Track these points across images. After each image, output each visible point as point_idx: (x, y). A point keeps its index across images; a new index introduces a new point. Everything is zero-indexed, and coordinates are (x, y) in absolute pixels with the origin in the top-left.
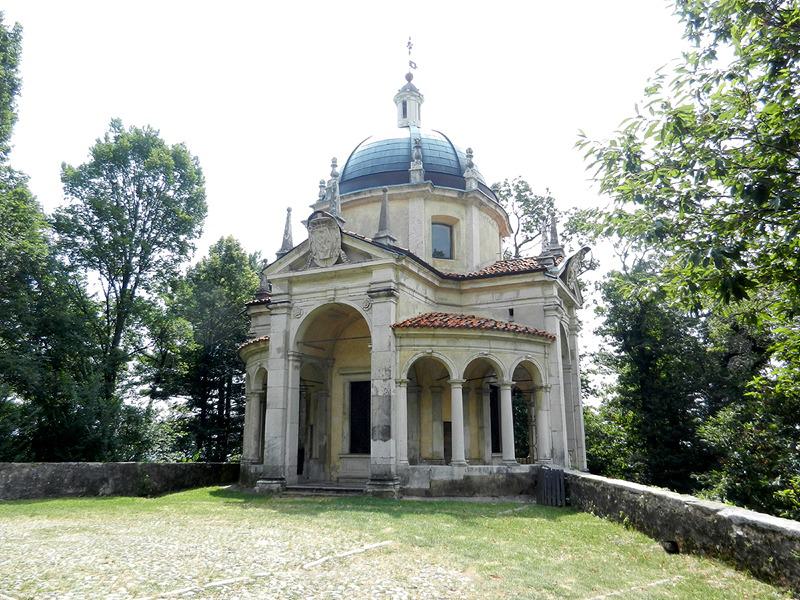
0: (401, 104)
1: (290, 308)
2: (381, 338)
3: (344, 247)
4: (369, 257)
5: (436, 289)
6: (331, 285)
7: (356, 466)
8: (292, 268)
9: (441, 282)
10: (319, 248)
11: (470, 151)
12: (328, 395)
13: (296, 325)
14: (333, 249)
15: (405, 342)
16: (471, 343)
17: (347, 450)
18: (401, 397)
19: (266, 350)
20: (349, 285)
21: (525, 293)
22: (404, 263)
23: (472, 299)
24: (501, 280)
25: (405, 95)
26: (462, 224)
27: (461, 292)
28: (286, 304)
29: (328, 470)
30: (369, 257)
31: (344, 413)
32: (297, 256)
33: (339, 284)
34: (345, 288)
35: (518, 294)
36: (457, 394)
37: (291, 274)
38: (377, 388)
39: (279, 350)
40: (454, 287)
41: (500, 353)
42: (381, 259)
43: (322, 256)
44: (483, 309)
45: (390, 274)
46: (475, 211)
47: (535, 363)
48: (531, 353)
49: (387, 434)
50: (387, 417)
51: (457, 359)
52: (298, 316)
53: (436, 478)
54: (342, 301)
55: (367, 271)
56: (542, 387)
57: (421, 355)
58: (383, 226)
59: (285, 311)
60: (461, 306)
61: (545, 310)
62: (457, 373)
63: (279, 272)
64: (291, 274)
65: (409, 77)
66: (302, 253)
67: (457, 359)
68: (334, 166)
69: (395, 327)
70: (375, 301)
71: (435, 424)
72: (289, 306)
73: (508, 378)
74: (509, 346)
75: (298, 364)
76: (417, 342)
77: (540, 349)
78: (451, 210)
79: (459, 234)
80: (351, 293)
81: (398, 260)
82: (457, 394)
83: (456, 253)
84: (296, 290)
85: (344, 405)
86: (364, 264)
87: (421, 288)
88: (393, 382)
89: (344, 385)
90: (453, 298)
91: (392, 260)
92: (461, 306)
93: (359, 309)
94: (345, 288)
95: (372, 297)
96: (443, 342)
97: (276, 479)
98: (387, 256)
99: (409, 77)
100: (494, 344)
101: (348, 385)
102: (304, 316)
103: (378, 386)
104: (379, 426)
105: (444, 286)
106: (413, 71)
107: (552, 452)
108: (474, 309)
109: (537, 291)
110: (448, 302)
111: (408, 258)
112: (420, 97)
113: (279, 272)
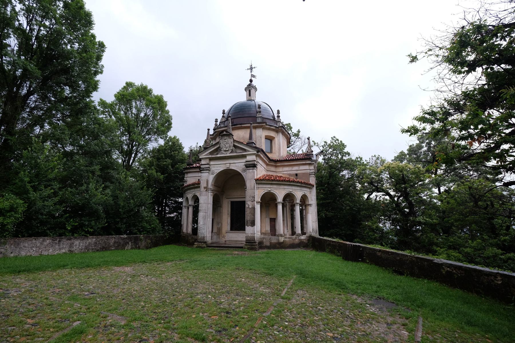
0: (248, 91)
1: (210, 170)
2: (250, 183)
3: (234, 146)
4: (245, 150)
5: (267, 165)
7: (239, 237)
9: (269, 162)
10: (223, 146)
11: (278, 112)
12: (221, 207)
14: (230, 147)
15: (260, 186)
18: (258, 207)
19: (199, 187)
21: (302, 167)
22: (260, 153)
23: (280, 169)
24: (292, 162)
25: (250, 88)
26: (276, 139)
27: (276, 166)
28: (208, 169)
29: (221, 237)
31: (228, 214)
32: (213, 149)
33: (231, 161)
35: (299, 168)
36: (280, 207)
37: (210, 156)
38: (249, 204)
39: (205, 188)
40: (274, 164)
41: (296, 191)
42: (249, 151)
43: (225, 149)
45: (253, 158)
46: (281, 135)
47: (307, 195)
48: (306, 191)
49: (253, 224)
50: (253, 217)
51: (280, 193)
52: (213, 174)
53: (272, 242)
55: (244, 156)
56: (309, 205)
57: (266, 191)
58: (251, 137)
59: (208, 171)
60: (276, 172)
61: (310, 175)
62: (280, 199)
63: (205, 156)
65: (251, 81)
66: (215, 148)
67: (280, 193)
68: (224, 113)
69: (256, 180)
71: (267, 219)
72: (208, 169)
73: (298, 201)
74: (298, 188)
75: (212, 194)
77: (308, 190)
78: (272, 134)
79: (275, 143)
80: (238, 165)
81: (258, 152)
82: (280, 207)
83: (273, 151)
84: (212, 163)
85: (228, 211)
88: (255, 202)
89: (228, 203)
90: (273, 169)
91: (256, 152)
92: (276, 172)
93: (240, 172)
95: (247, 167)
96: (275, 186)
97: (203, 242)
98: (253, 151)
99: (251, 81)
100: (294, 188)
101: (230, 203)
102: (215, 175)
103: (250, 204)
104: (250, 220)
105: (270, 163)
106: (253, 79)
107: (313, 229)
110: (271, 170)
111: (262, 153)
112: (256, 89)
113: (205, 156)
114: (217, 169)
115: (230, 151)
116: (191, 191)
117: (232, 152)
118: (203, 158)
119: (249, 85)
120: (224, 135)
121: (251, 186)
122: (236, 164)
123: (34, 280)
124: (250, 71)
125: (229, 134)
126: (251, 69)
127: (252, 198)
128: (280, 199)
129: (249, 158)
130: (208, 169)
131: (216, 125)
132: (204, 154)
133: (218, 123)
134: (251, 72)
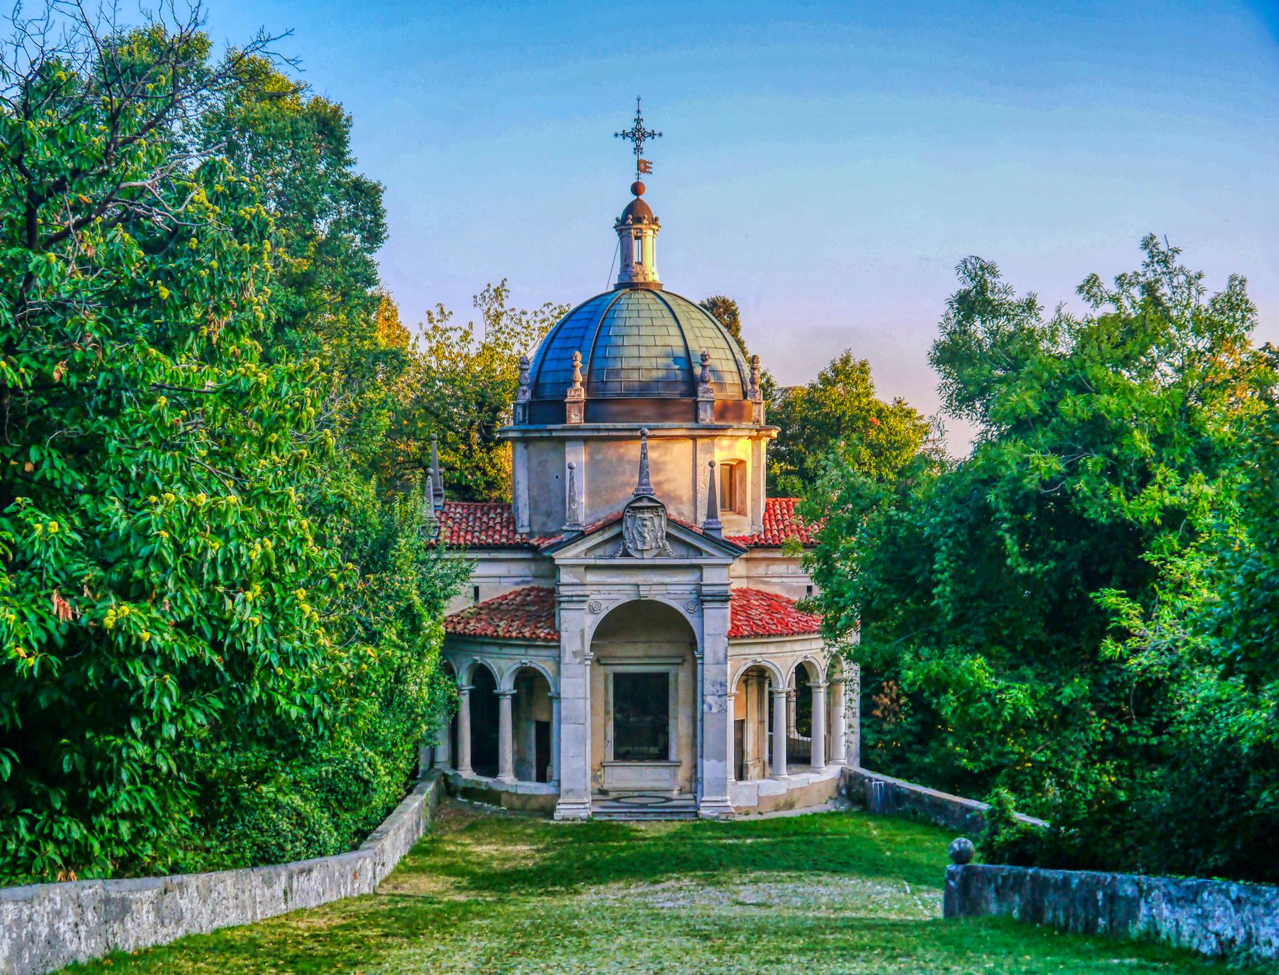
4: (699, 552)
6: (639, 578)
16: (797, 647)
17: (610, 757)
20: (667, 579)
23: (761, 570)
30: (699, 552)
31: (607, 712)
34: (663, 584)
39: (575, 654)
42: (712, 556)
44: (775, 584)
57: (750, 664)
65: (637, 189)
70: (707, 605)
76: (746, 650)
85: (606, 703)
86: (695, 561)
93: (682, 610)
94: (663, 584)
96: (772, 649)
99: (637, 189)
101: (611, 677)
103: (713, 703)
106: (644, 179)
108: (766, 583)
114: (607, 596)
115: (655, 552)
116: (514, 651)
118: (565, 566)
119: (630, 209)
121: (715, 653)
122: (669, 587)
123: (29, 901)
124: (629, 144)
125: (656, 507)
126: (638, 135)
127: (718, 687)
128: (785, 682)
129: (710, 576)
132: (570, 554)
134: (638, 150)
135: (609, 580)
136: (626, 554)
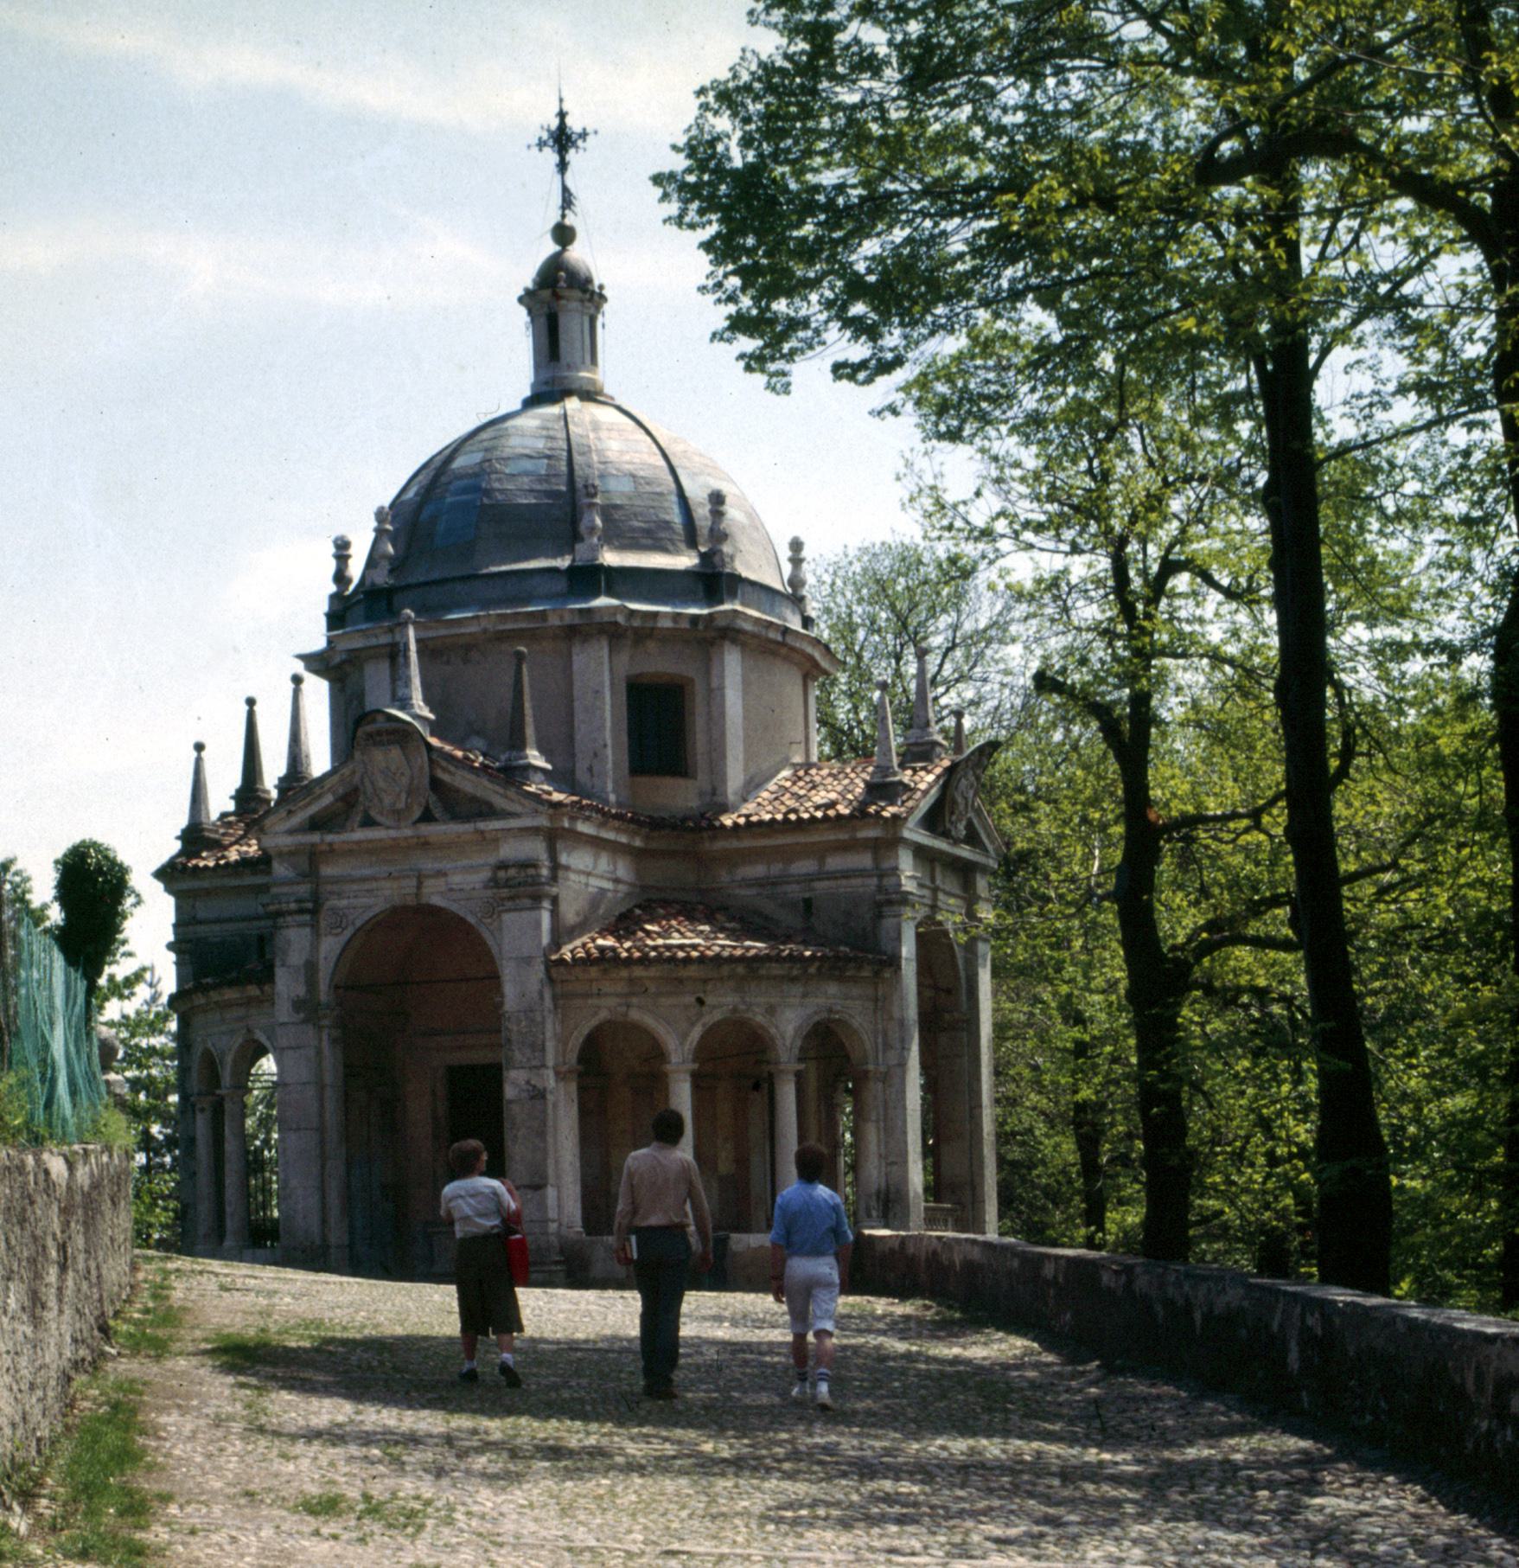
0: (543, 321)
3: (436, 784)
8: (315, 824)
13: (330, 946)
33: (428, 864)
39: (298, 1005)
54: (437, 901)
59: (307, 917)
63: (291, 832)
64: (315, 838)
65: (563, 234)
84: (327, 870)
87: (604, 863)
99: (563, 234)
109: (865, 860)
113: (291, 832)
115: (417, 813)
117: (427, 817)
120: (379, 733)
126: (562, 139)
130: (312, 909)
131: (340, 577)
133: (356, 569)
135: (358, 873)
136: (368, 822)
